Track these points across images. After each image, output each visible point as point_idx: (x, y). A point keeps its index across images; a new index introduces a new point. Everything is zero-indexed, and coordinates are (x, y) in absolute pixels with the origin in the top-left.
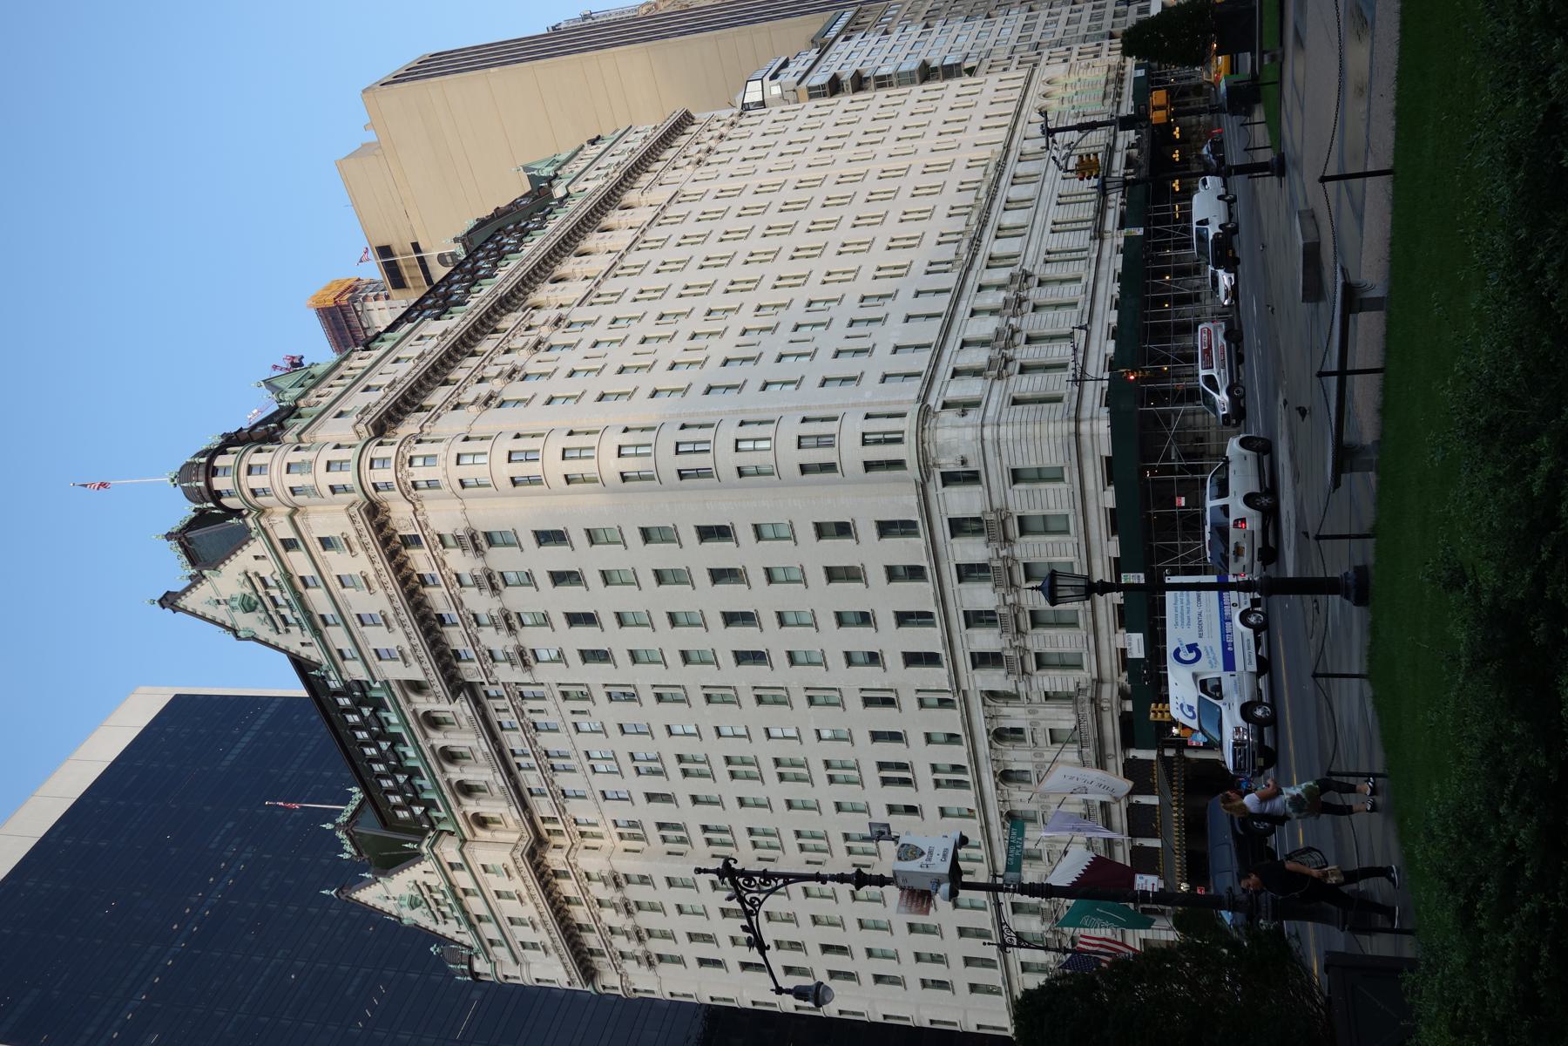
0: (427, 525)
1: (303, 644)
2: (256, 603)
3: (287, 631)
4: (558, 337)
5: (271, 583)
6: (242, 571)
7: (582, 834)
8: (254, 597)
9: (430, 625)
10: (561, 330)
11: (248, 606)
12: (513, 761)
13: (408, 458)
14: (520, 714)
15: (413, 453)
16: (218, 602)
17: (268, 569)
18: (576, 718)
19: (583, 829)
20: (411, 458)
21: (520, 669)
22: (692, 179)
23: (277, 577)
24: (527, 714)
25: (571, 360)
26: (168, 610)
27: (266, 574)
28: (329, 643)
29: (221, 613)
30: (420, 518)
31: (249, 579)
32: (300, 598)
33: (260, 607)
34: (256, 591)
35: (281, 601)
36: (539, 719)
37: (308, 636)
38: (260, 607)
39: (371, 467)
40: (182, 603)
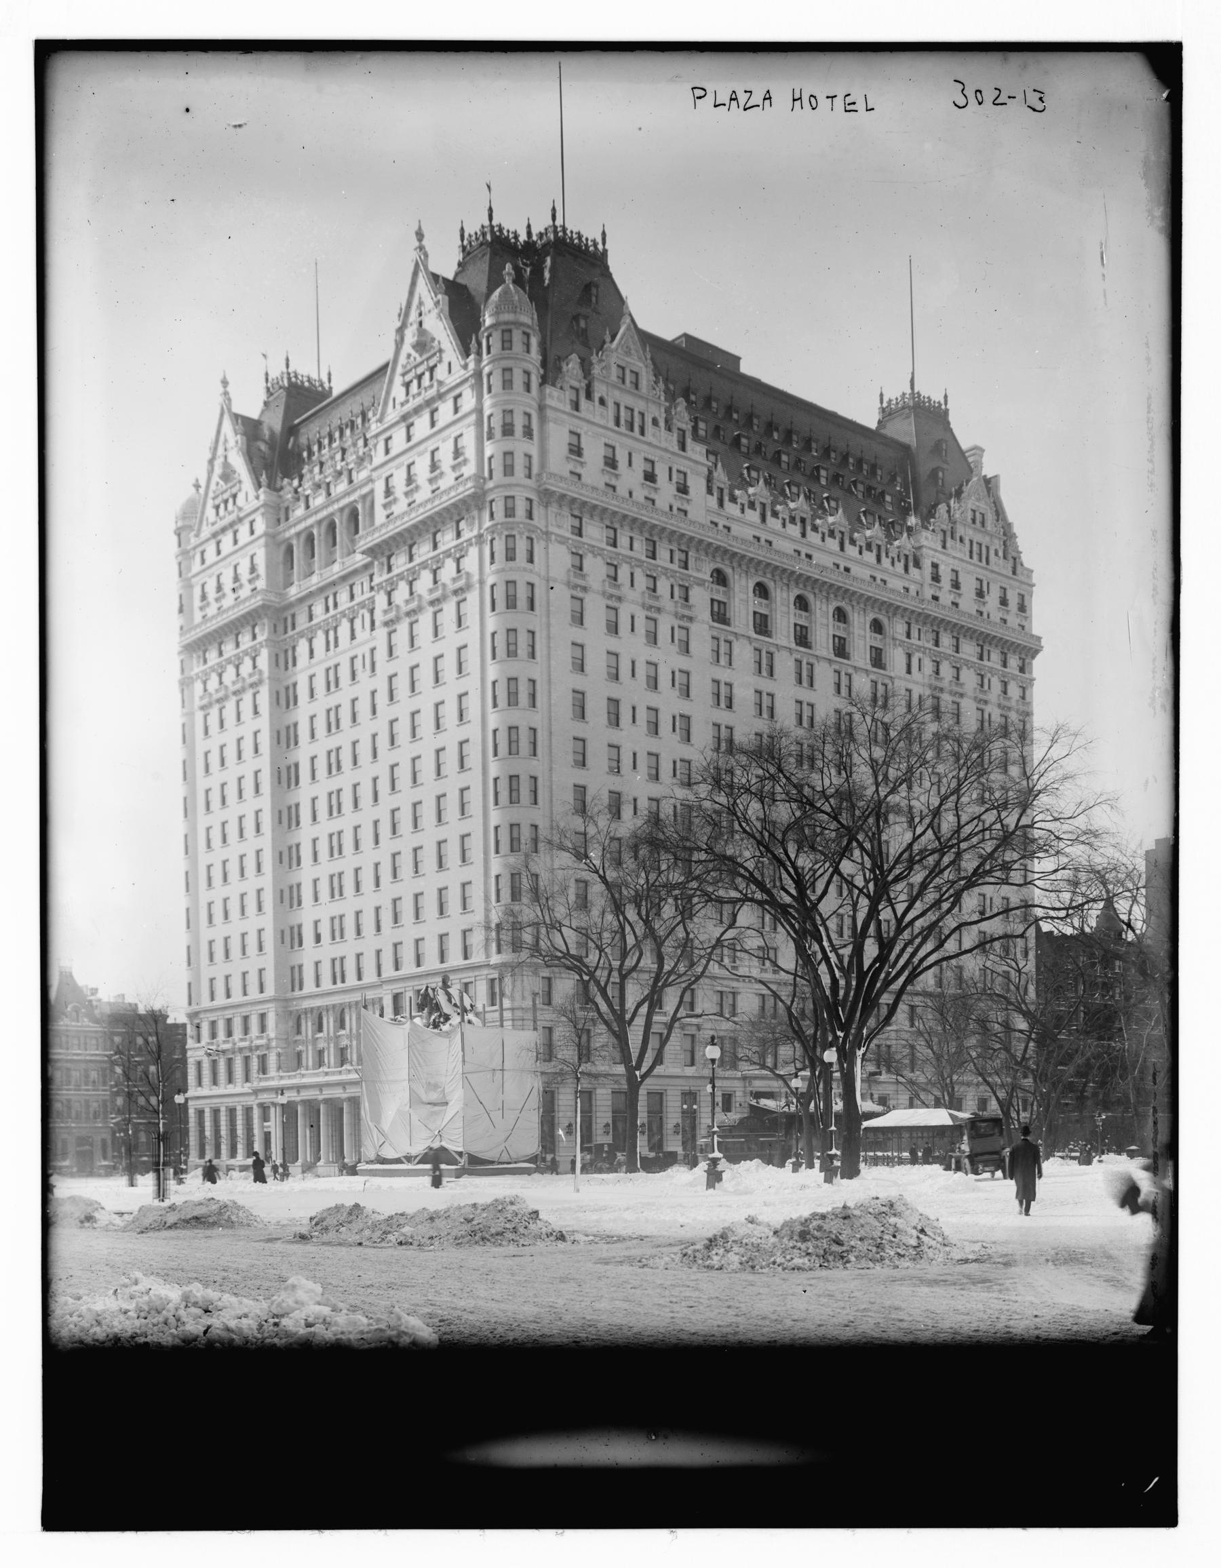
4: (665, 625)
7: (286, 651)
9: (407, 539)
10: (676, 623)
12: (330, 593)
13: (514, 533)
14: (362, 605)
15: (517, 537)
18: (360, 658)
19: (290, 653)
20: (514, 536)
22: (910, 686)
24: (361, 612)
25: (632, 646)
28: (396, 429)
36: (358, 623)
39: (506, 498)
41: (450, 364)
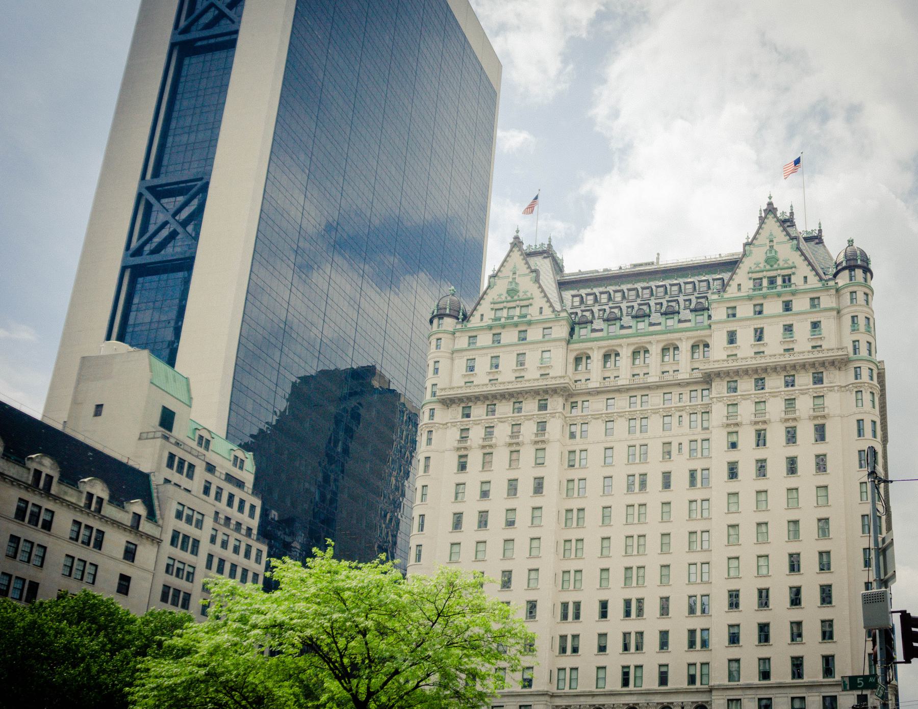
1: (482, 315)
2: (512, 297)
3: (492, 309)
5: (524, 311)
6: (533, 296)
8: (516, 298)
11: (512, 292)
16: (514, 273)
17: (533, 312)
21: (456, 445)
23: (529, 317)
26: (512, 240)
27: (531, 310)
29: (507, 271)
30: (557, 415)
31: (529, 299)
32: (516, 325)
33: (509, 298)
34: (520, 300)
35: (512, 312)
37: (487, 321)
38: (509, 298)
40: (516, 250)
41: (541, 308)
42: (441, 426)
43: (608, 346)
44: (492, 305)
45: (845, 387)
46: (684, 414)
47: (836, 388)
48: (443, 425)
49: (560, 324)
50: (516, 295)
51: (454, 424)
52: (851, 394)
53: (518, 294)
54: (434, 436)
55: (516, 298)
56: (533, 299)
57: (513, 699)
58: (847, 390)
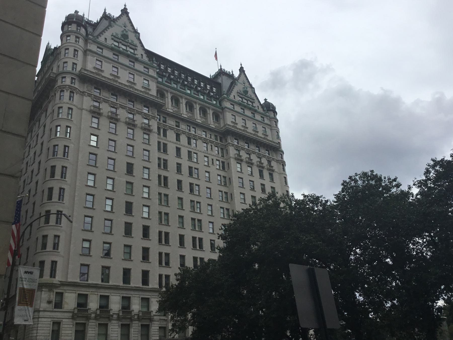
0: (153, 119)
42: (79, 92)
43: (175, 94)
44: (113, 37)
45: (277, 160)
46: (213, 145)
47: (275, 160)
48: (81, 92)
49: (154, 69)
50: (127, 39)
51: (89, 95)
52: (280, 164)
53: (128, 40)
54: (76, 97)
55: (127, 40)
56: (137, 47)
57: (136, 293)
58: (278, 162)
